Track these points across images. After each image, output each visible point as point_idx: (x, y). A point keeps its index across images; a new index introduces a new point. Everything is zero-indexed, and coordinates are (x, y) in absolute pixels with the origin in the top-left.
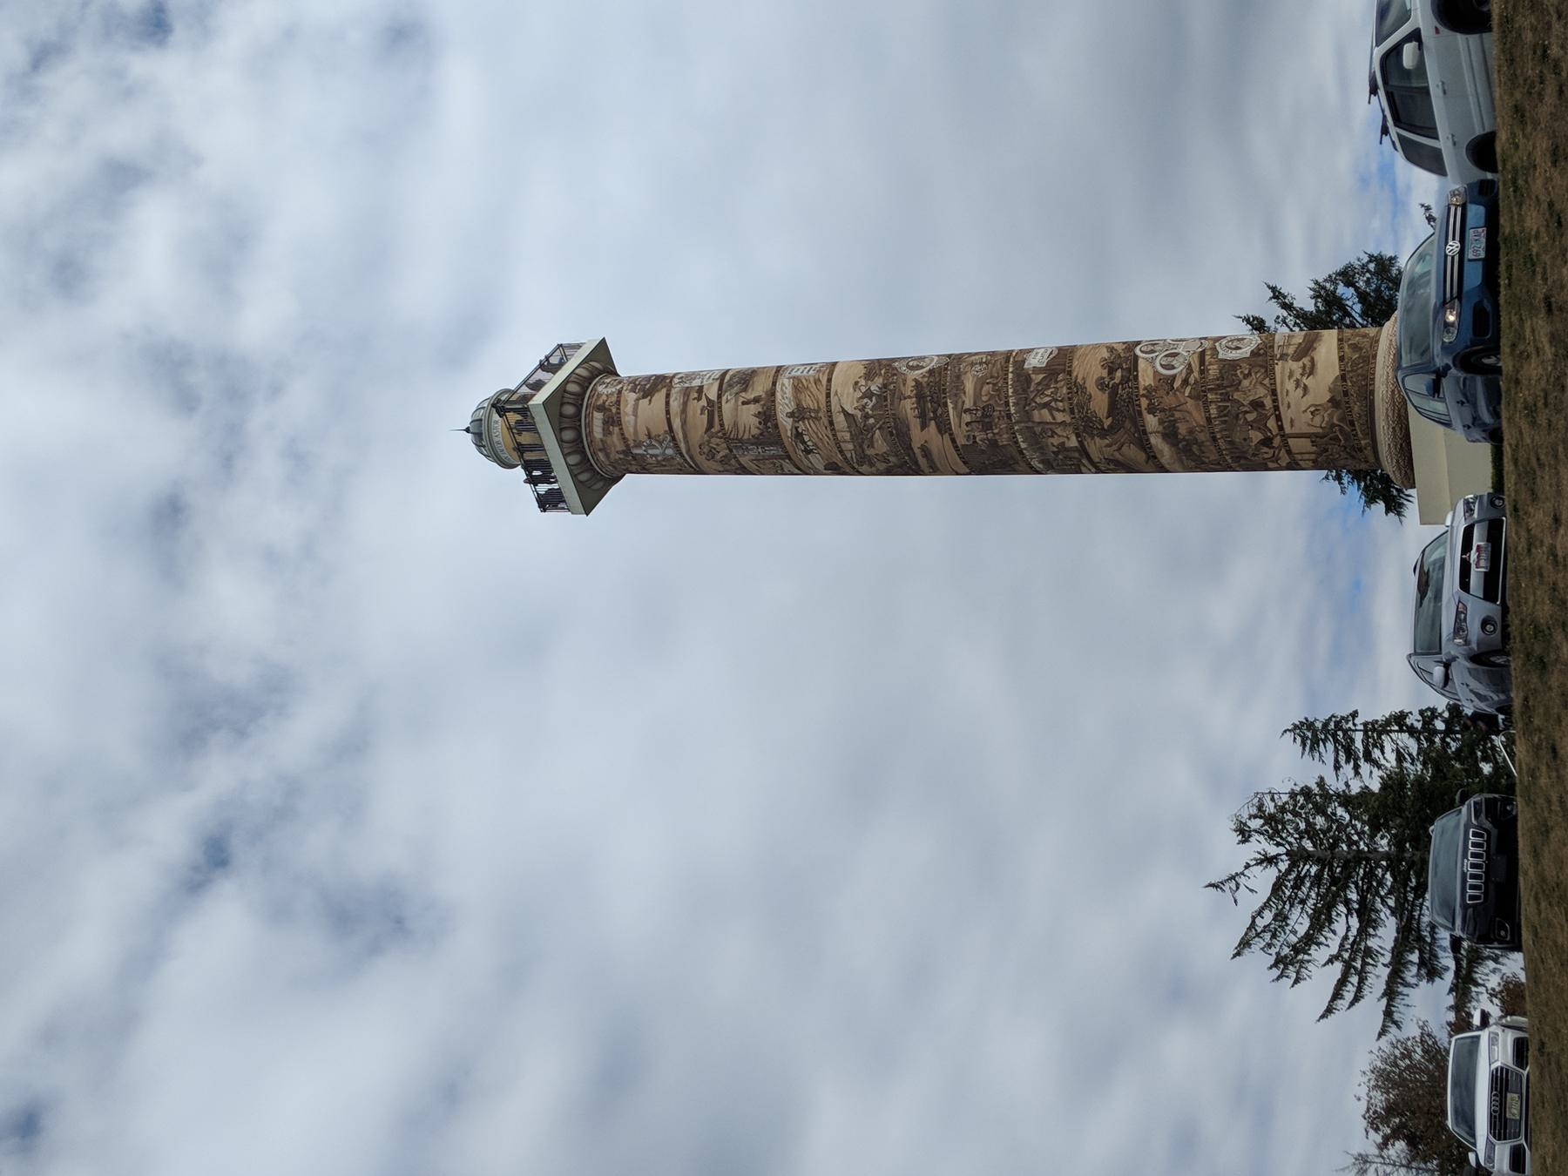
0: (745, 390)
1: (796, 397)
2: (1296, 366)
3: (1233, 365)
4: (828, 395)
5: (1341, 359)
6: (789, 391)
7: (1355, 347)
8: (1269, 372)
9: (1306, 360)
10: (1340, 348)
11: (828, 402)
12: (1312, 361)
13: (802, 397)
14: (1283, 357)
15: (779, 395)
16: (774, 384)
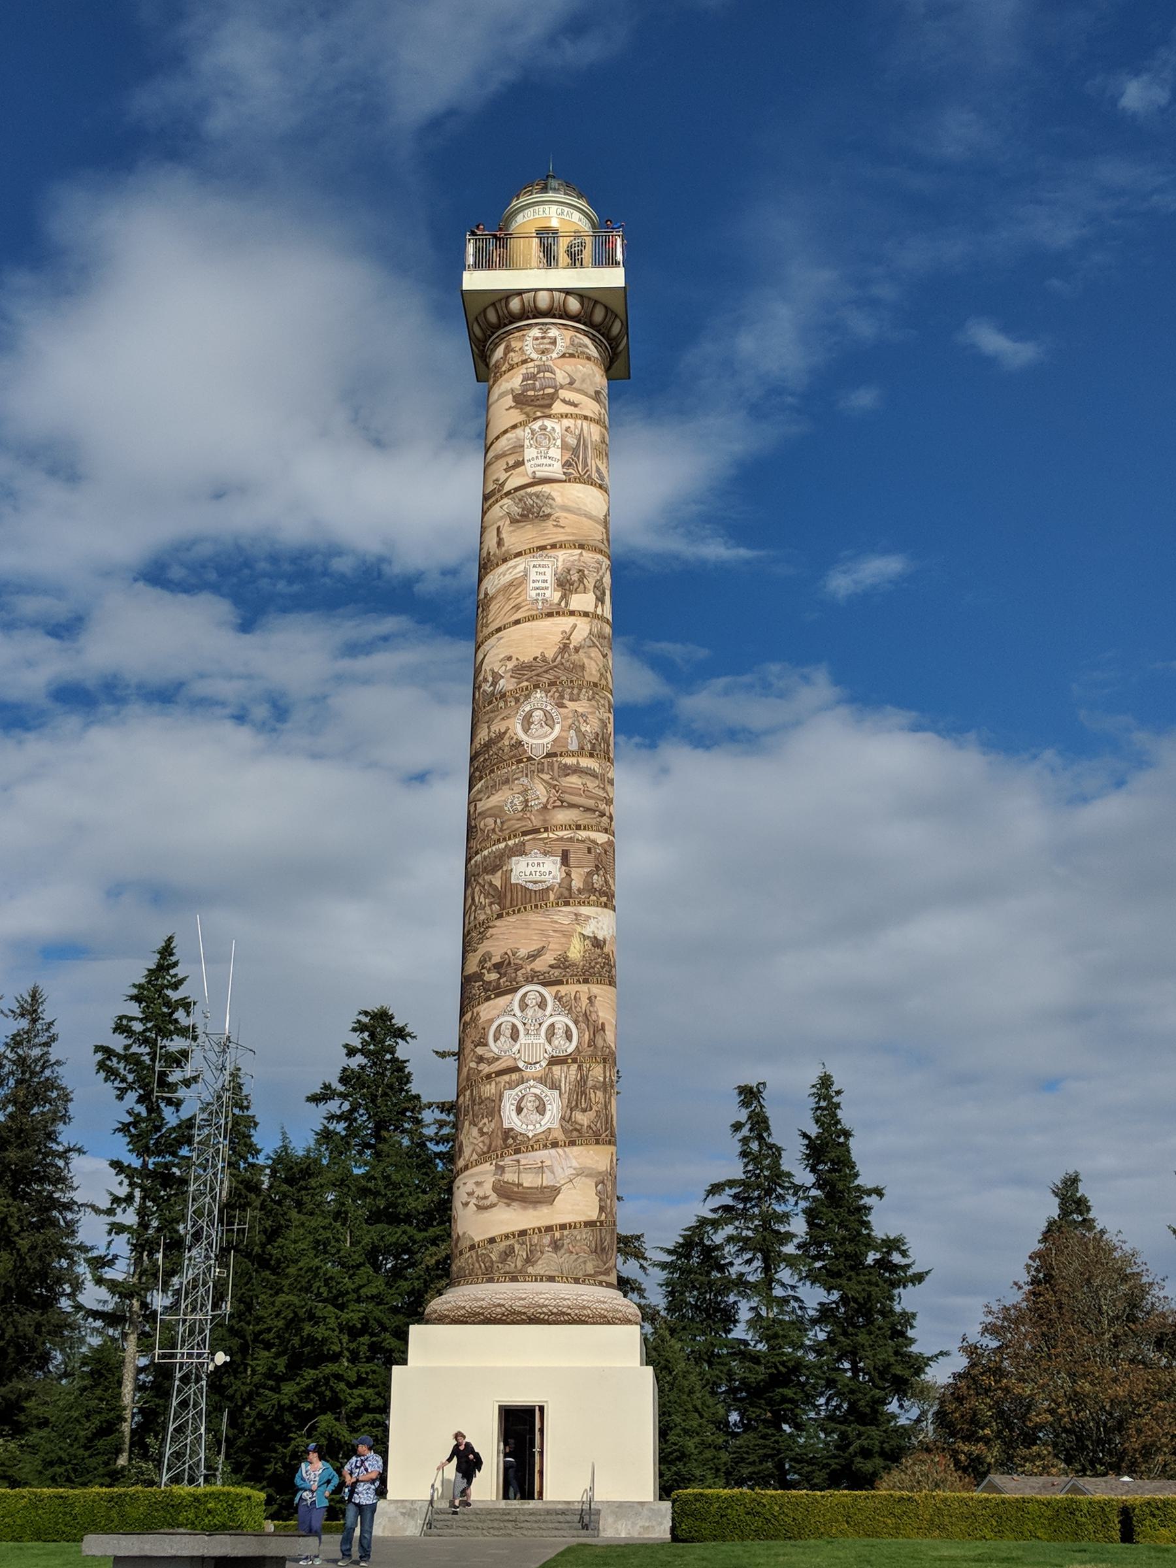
0: (514, 521)
1: (498, 591)
2: (487, 1189)
3: (494, 1110)
4: (499, 630)
5: (492, 1241)
6: (508, 577)
7: (508, 1253)
8: (484, 1157)
9: (493, 1198)
10: (507, 1237)
11: (493, 634)
12: (493, 1206)
13: (500, 598)
14: (501, 1169)
15: (503, 568)
16: (519, 554)
